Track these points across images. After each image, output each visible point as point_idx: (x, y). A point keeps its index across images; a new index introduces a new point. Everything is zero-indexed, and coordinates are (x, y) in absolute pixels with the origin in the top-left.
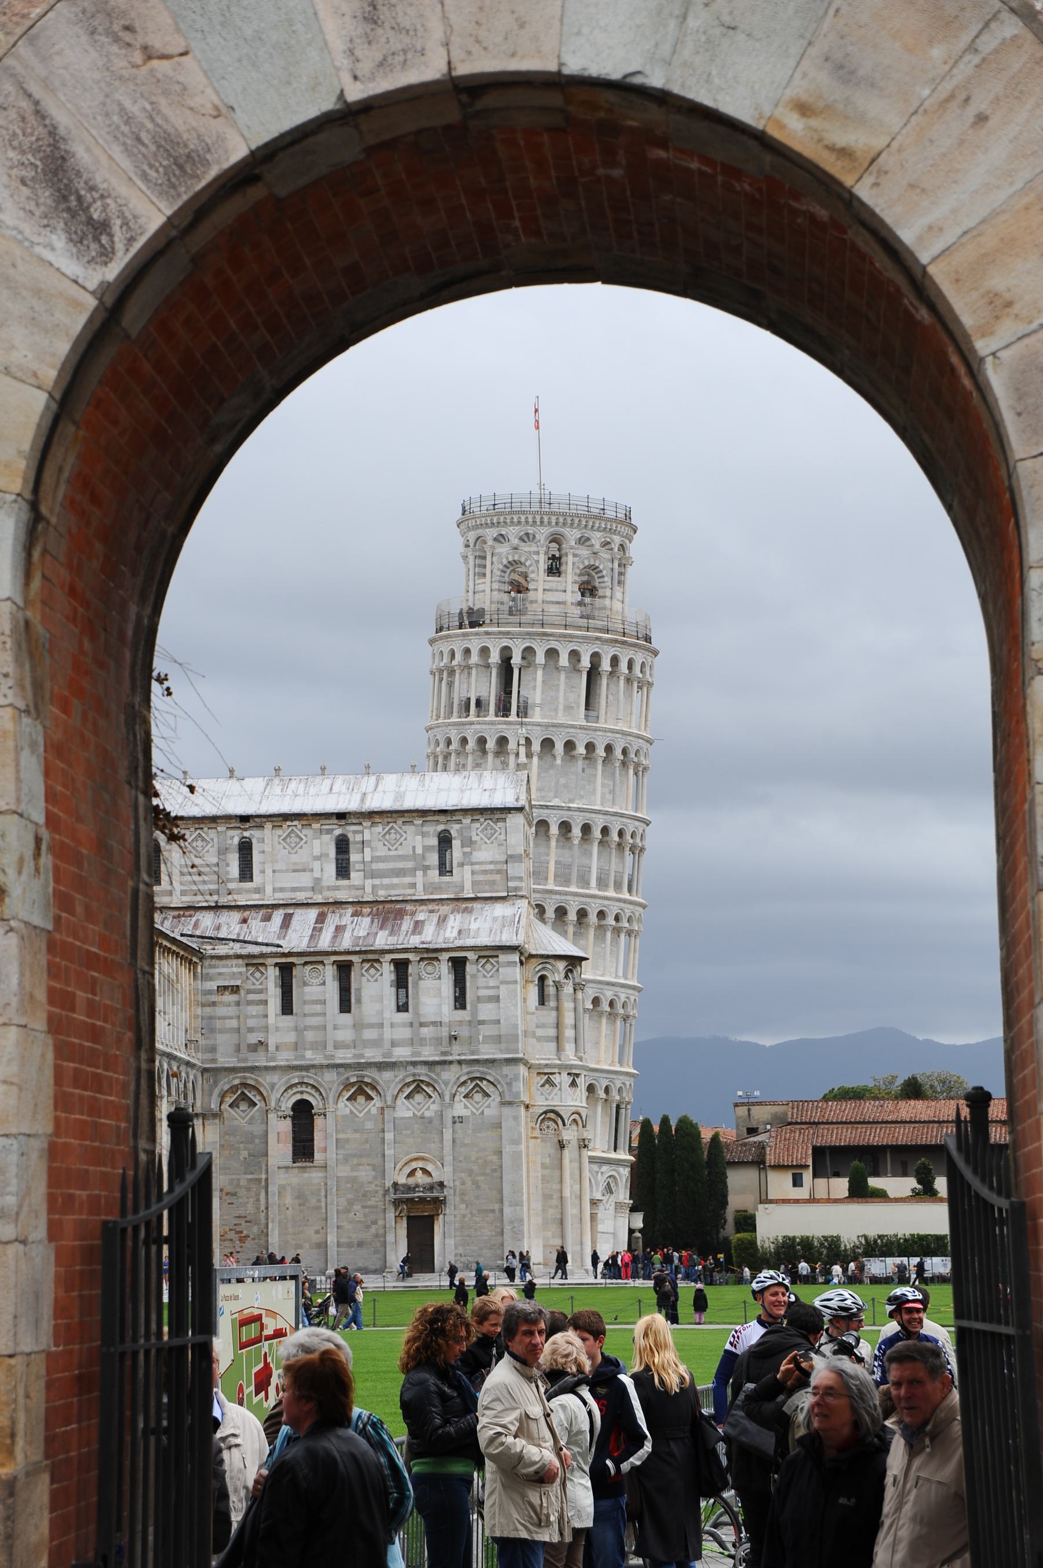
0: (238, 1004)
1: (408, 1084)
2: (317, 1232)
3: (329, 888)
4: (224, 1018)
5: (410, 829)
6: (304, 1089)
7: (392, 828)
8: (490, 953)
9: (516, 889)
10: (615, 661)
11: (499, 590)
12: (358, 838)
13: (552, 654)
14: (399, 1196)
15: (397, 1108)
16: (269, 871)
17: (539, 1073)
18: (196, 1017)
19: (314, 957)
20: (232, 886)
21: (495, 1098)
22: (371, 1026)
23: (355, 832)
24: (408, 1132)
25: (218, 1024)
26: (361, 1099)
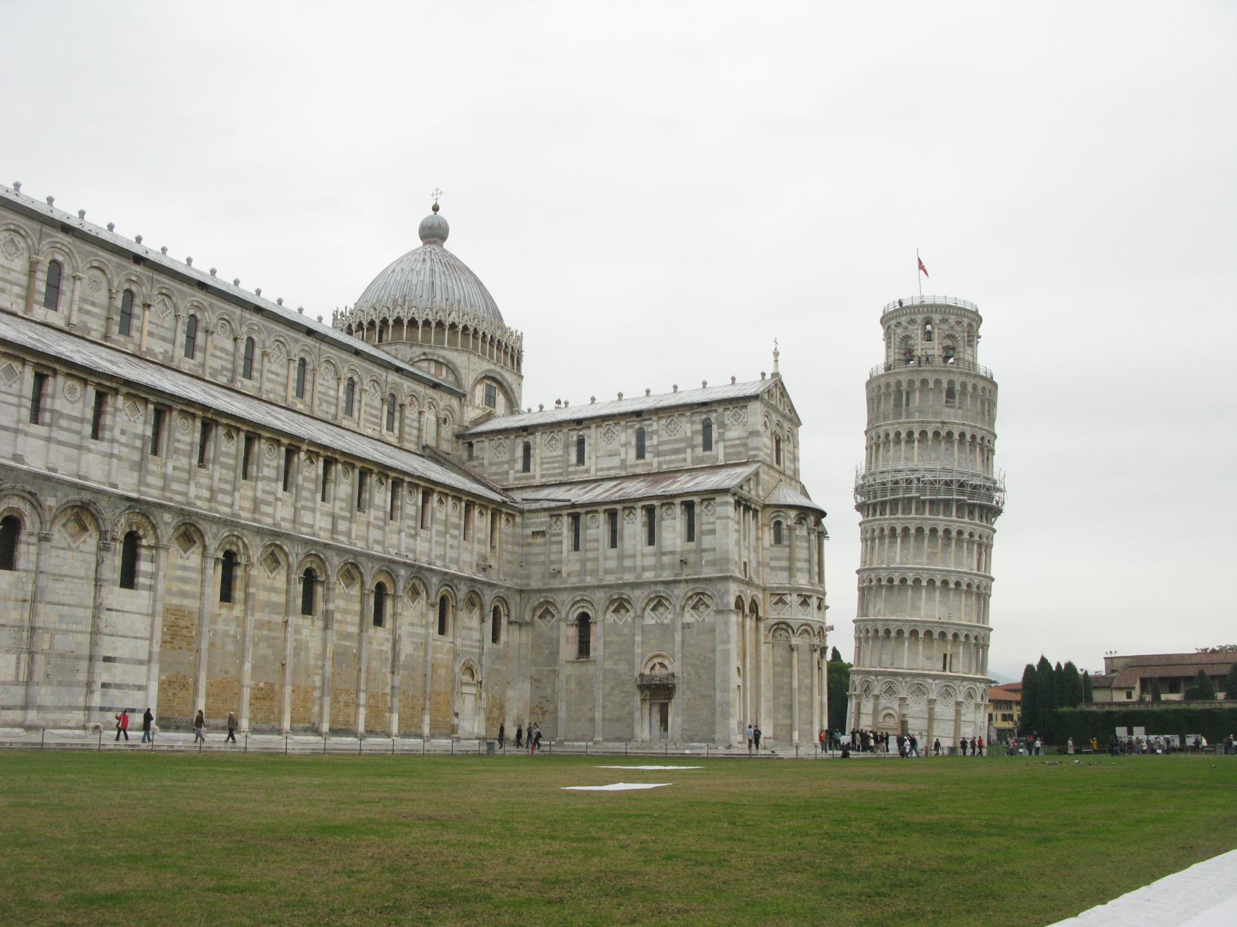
0: (545, 544)
1: (652, 600)
2: (590, 710)
3: (632, 466)
4: (534, 555)
5: (684, 419)
6: (584, 604)
7: (672, 420)
8: (710, 495)
9: (755, 456)
10: (964, 385)
11: (898, 353)
12: (650, 429)
13: (924, 382)
14: (644, 682)
15: (645, 618)
16: (593, 457)
17: (772, 594)
18: (512, 553)
19: (592, 507)
20: (571, 469)
21: (713, 608)
22: (629, 556)
23: (648, 425)
24: (652, 635)
25: (532, 559)
26: (623, 611)
